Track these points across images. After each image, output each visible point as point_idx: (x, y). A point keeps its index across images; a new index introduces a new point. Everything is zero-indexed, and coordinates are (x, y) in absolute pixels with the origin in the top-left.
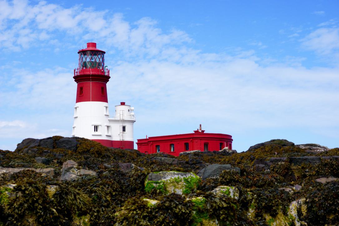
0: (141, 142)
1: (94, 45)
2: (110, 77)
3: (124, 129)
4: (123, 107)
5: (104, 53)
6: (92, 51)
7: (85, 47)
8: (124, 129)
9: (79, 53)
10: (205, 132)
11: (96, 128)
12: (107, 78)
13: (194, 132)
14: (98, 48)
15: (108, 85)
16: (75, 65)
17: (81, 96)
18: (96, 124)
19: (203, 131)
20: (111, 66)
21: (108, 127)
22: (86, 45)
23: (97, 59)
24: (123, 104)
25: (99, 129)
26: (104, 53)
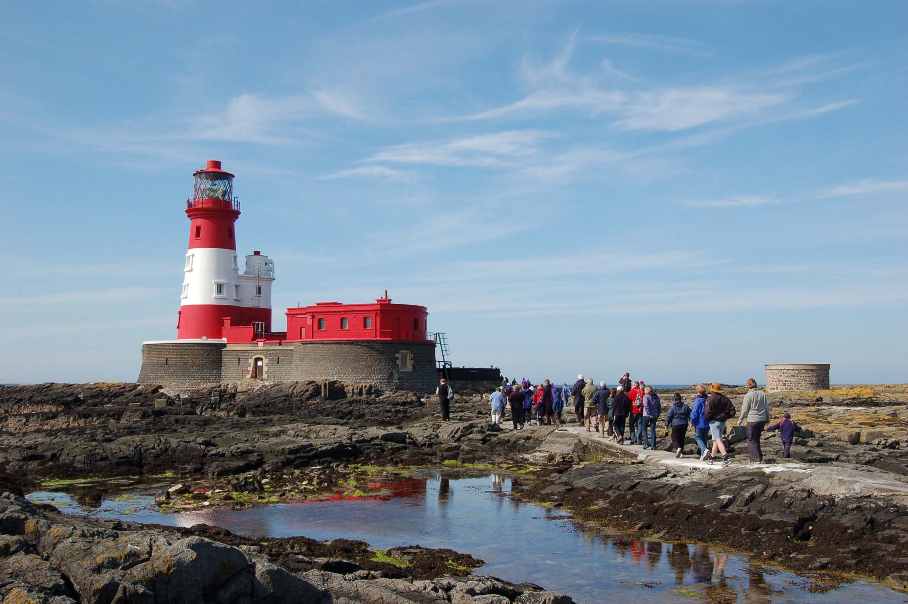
0: (292, 314)
1: (217, 164)
3: (259, 290)
4: (257, 257)
5: (233, 176)
8: (259, 290)
9: (194, 175)
11: (220, 287)
12: (236, 214)
14: (224, 168)
15: (238, 225)
16: (189, 190)
19: (390, 300)
20: (241, 195)
21: (236, 286)
22: (206, 164)
23: (221, 186)
25: (224, 289)
26: (233, 176)
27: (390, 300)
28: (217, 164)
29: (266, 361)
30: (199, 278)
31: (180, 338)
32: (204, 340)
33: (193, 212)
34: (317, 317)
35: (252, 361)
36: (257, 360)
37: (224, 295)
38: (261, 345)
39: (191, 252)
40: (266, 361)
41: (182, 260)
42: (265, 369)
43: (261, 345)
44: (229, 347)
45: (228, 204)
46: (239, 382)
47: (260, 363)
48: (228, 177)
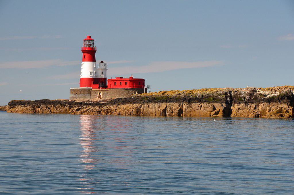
1: (90, 37)
2: (96, 51)
6: (90, 39)
7: (86, 38)
10: (133, 78)
11: (91, 73)
13: (129, 78)
14: (92, 38)
17: (84, 59)
18: (91, 71)
19: (133, 77)
20: (97, 45)
23: (91, 43)
24: (102, 62)
25: (92, 73)
27: (133, 77)
28: (90, 37)
29: (102, 93)
30: (87, 70)
31: (81, 86)
32: (86, 88)
33: (84, 52)
34: (114, 82)
35: (98, 93)
36: (100, 93)
37: (92, 75)
38: (101, 89)
39: (83, 62)
40: (102, 93)
41: (81, 65)
42: (102, 95)
43: (101, 89)
44: (93, 90)
45: (93, 48)
46: (95, 99)
47: (100, 94)
48: (93, 40)
